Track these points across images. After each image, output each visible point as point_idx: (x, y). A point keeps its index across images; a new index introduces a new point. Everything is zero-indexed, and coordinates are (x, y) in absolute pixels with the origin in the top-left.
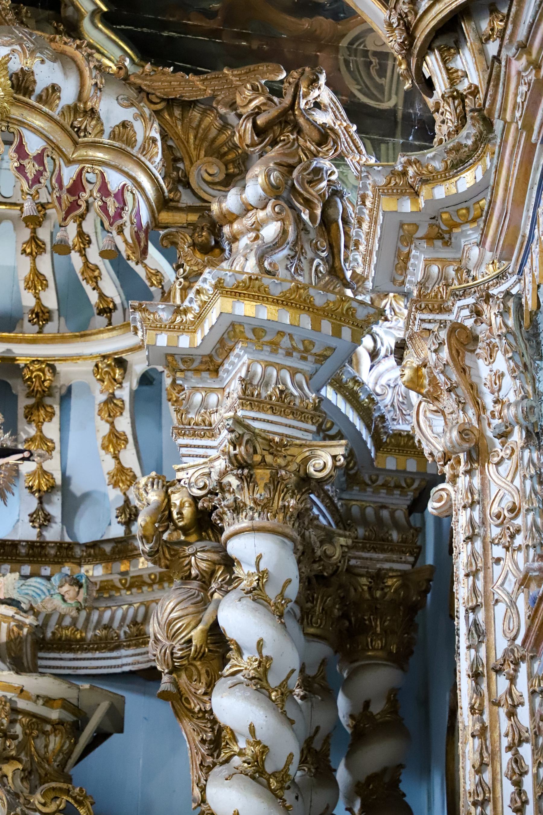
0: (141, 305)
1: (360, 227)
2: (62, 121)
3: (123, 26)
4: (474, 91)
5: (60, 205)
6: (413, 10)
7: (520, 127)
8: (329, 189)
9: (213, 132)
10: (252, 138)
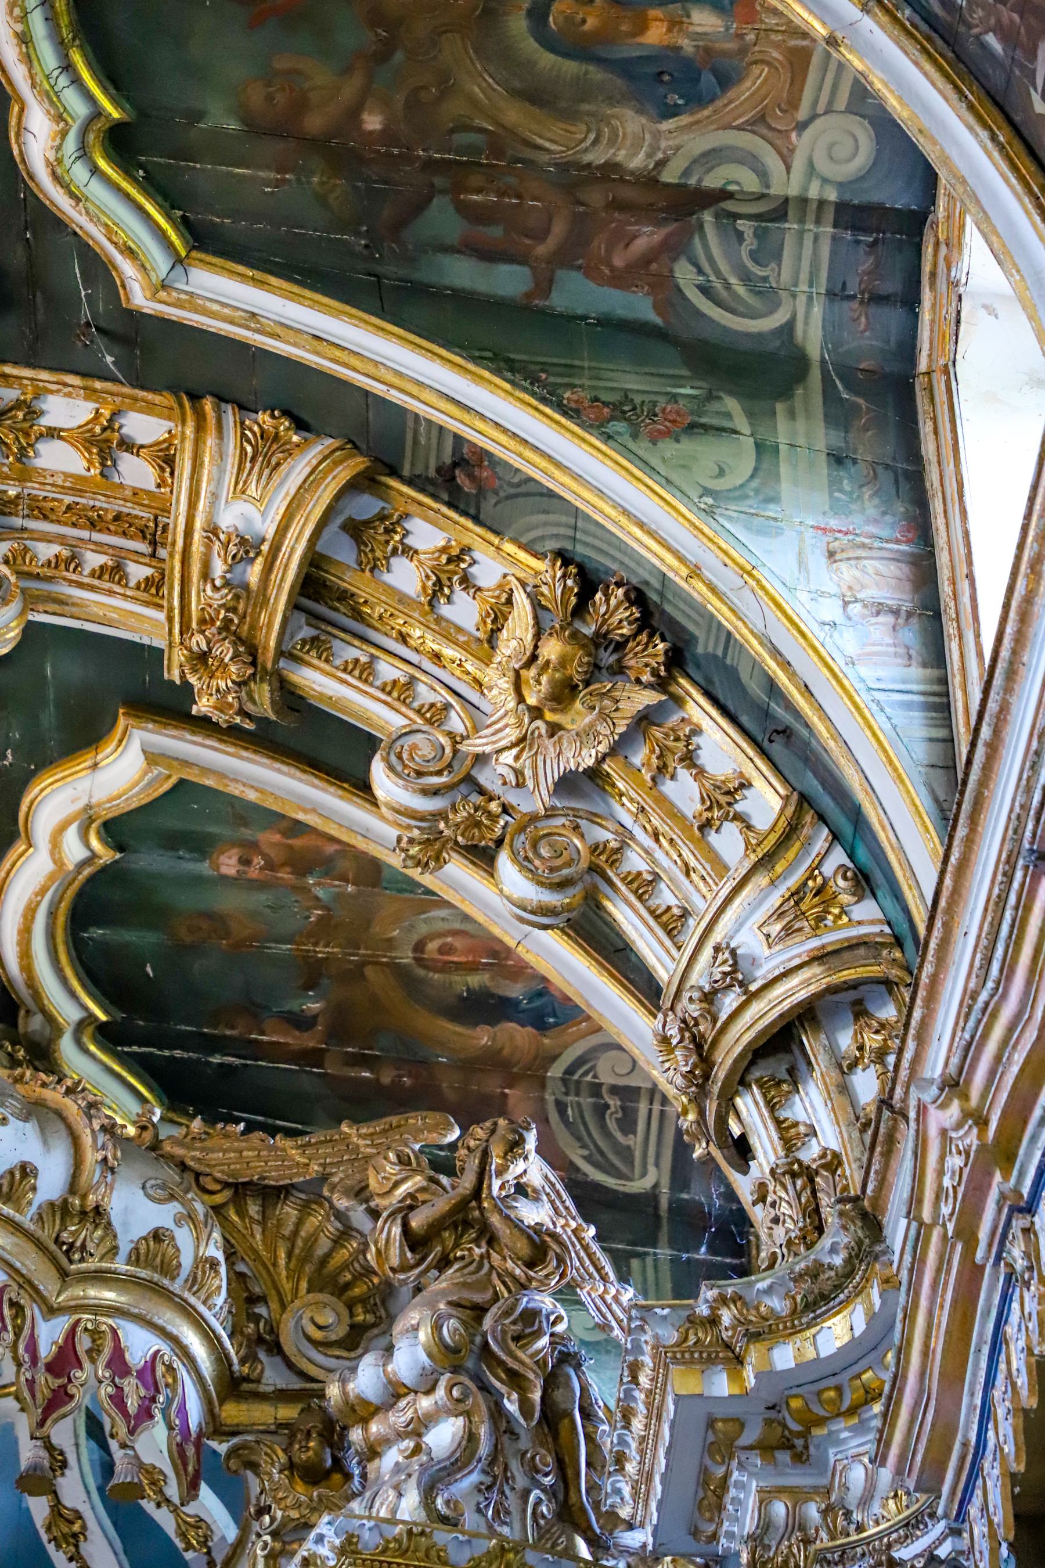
1: (627, 1426)
2: (39, 1233)
3: (135, 1048)
4: (831, 1162)
5: (33, 1396)
6: (709, 1012)
7: (950, 1234)
8: (553, 1352)
9: (324, 1245)
10: (402, 1253)
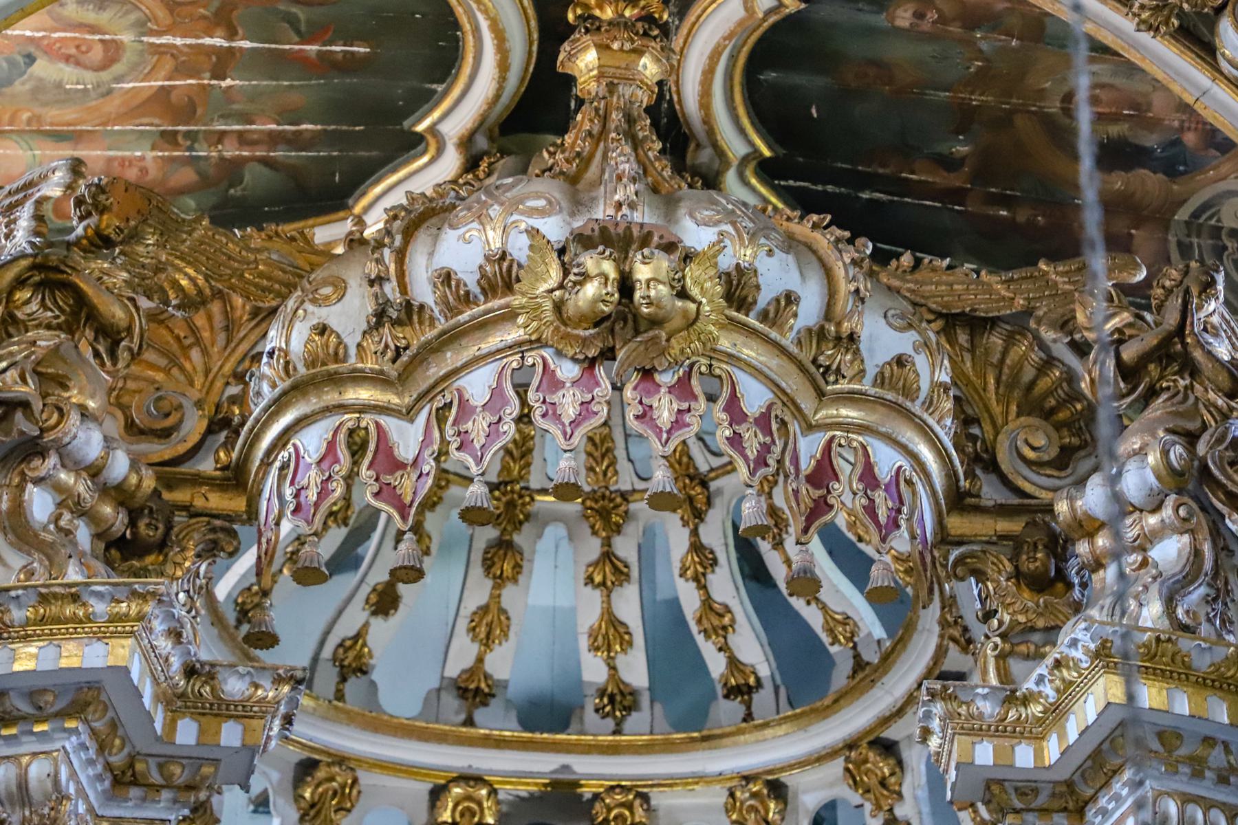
0: (945, 688)
5: (798, 505)
